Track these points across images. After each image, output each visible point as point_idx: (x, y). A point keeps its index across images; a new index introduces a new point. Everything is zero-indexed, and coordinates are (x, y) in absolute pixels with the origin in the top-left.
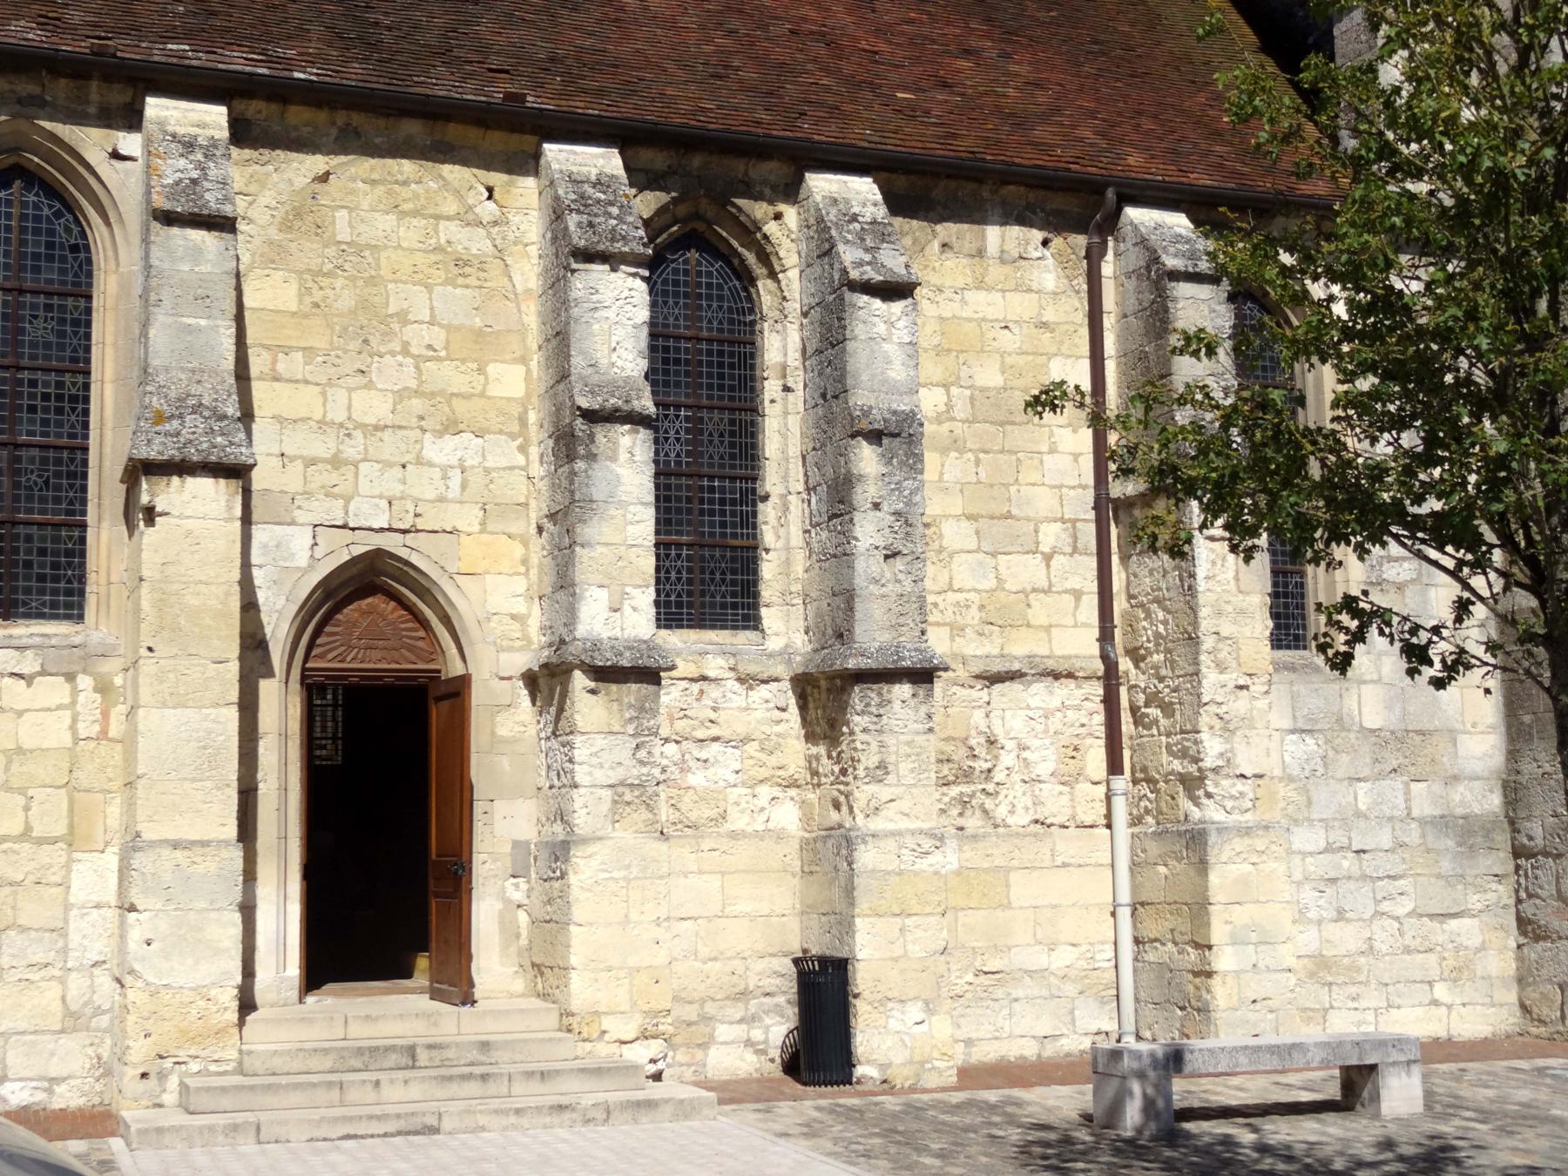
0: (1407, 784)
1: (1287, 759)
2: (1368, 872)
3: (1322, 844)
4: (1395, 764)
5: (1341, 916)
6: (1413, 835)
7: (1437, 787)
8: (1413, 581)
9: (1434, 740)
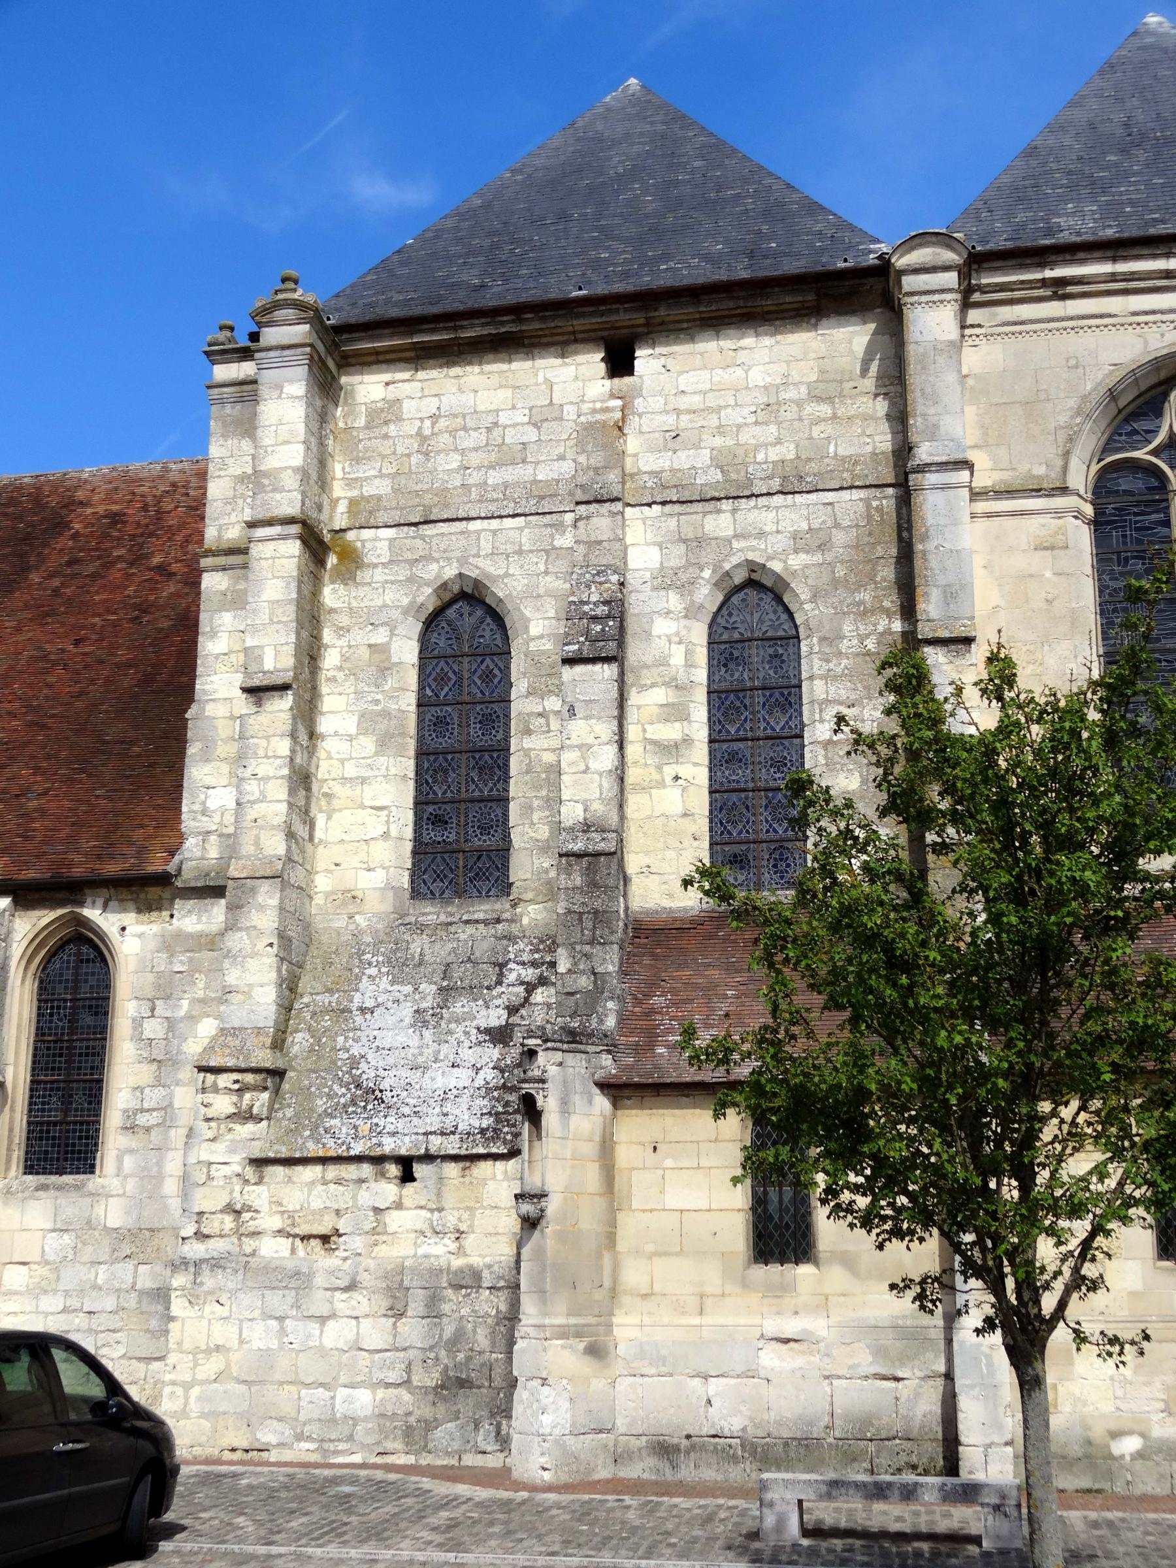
0: (136, 1267)
1: (46, 1248)
2: (94, 1327)
3: (61, 1307)
4: (128, 1252)
6: (132, 1301)
7: (158, 1268)
8: (158, 1125)
9: (161, 1235)
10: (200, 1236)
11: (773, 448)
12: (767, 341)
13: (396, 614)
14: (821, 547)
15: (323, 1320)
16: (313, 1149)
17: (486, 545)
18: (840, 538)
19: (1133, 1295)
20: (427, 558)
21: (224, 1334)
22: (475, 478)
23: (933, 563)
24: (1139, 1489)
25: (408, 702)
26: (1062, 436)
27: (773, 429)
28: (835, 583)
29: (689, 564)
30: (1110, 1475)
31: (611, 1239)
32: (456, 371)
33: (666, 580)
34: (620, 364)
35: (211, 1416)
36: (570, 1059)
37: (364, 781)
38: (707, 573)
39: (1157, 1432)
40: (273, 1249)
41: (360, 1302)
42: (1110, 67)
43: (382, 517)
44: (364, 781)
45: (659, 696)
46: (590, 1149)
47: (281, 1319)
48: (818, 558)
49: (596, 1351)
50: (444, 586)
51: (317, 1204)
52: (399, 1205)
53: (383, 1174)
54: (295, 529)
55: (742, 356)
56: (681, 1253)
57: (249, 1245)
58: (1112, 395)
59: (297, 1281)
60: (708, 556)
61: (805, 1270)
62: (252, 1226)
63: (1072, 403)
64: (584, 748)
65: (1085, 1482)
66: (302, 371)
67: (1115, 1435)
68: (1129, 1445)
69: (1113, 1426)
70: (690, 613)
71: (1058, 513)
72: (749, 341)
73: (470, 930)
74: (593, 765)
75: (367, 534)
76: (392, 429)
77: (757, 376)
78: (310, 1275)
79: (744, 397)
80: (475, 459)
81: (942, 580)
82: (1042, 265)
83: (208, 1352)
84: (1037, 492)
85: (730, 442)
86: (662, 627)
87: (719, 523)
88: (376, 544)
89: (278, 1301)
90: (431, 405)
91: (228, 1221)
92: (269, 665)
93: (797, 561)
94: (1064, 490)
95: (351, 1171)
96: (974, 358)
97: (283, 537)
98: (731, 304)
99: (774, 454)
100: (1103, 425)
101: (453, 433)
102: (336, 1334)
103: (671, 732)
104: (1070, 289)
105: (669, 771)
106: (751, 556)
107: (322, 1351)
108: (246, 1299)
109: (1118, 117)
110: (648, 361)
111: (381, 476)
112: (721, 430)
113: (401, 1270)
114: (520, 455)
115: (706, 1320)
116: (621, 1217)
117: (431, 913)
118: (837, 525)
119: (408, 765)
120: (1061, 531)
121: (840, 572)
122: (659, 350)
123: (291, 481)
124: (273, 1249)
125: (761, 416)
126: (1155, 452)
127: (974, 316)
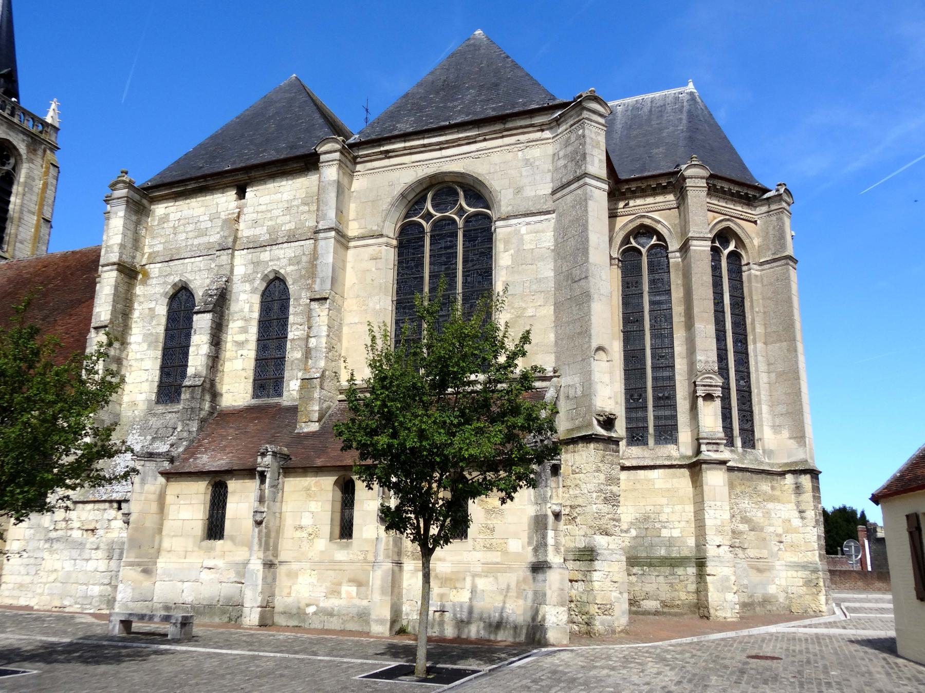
5: (28, 574)
10: (55, 530)
11: (288, 224)
12: (290, 182)
13: (158, 296)
14: (298, 263)
15: (87, 560)
16: (91, 498)
17: (189, 269)
18: (304, 259)
19: (322, 552)
20: (170, 274)
21: (57, 565)
22: (190, 242)
23: (319, 269)
24: (312, 626)
25: (161, 330)
26: (384, 213)
27: (288, 217)
28: (301, 277)
29: (254, 272)
30: (304, 621)
31: (160, 530)
32: (188, 201)
33: (247, 279)
34: (241, 194)
35: (51, 594)
36: (148, 464)
37: (142, 360)
38: (259, 275)
39: (322, 605)
40: (76, 534)
41: (100, 554)
42: (453, 55)
43: (158, 259)
44: (142, 360)
45: (240, 323)
46: (154, 497)
47: (75, 560)
48: (296, 267)
49: (147, 572)
50: (175, 284)
51: (91, 518)
52: (115, 519)
53: (111, 507)
54: (115, 267)
55: (281, 189)
56: (181, 536)
57: (69, 532)
58: (403, 195)
59: (80, 545)
60: (260, 269)
61: (221, 542)
62: (70, 526)
63: (389, 200)
64: (198, 346)
65: (296, 623)
66: (124, 207)
67: (308, 605)
68: (311, 610)
69: (307, 602)
70: (254, 291)
71: (379, 245)
72: (284, 183)
73: (170, 415)
74: (200, 352)
75: (152, 266)
76: (165, 225)
77: (286, 197)
78: (85, 544)
79: (280, 205)
80: (191, 235)
81: (321, 275)
82: (380, 146)
83: (52, 571)
84: (372, 237)
85: (273, 223)
86: (243, 297)
87: (265, 256)
88: (154, 270)
89: (75, 553)
90: (178, 215)
91: (64, 524)
92: (102, 319)
93: (290, 269)
94: (382, 236)
95: (102, 506)
96: (359, 184)
97: (112, 270)
98: (276, 169)
99: (287, 227)
100: (402, 207)
101: (184, 225)
102: (91, 565)
103: (241, 338)
104: (391, 154)
105: (240, 352)
106: (275, 268)
107: (86, 572)
108: (66, 553)
109: (443, 78)
110: (250, 193)
111: (160, 243)
112: (271, 219)
113: (113, 542)
114: (203, 233)
115: (186, 560)
116: (165, 522)
117: (161, 409)
118: (304, 254)
119: (159, 354)
120: (380, 252)
121: (303, 272)
122: (255, 188)
123: (116, 249)
124: (76, 534)
125: (285, 212)
126: (420, 218)
127: (359, 167)
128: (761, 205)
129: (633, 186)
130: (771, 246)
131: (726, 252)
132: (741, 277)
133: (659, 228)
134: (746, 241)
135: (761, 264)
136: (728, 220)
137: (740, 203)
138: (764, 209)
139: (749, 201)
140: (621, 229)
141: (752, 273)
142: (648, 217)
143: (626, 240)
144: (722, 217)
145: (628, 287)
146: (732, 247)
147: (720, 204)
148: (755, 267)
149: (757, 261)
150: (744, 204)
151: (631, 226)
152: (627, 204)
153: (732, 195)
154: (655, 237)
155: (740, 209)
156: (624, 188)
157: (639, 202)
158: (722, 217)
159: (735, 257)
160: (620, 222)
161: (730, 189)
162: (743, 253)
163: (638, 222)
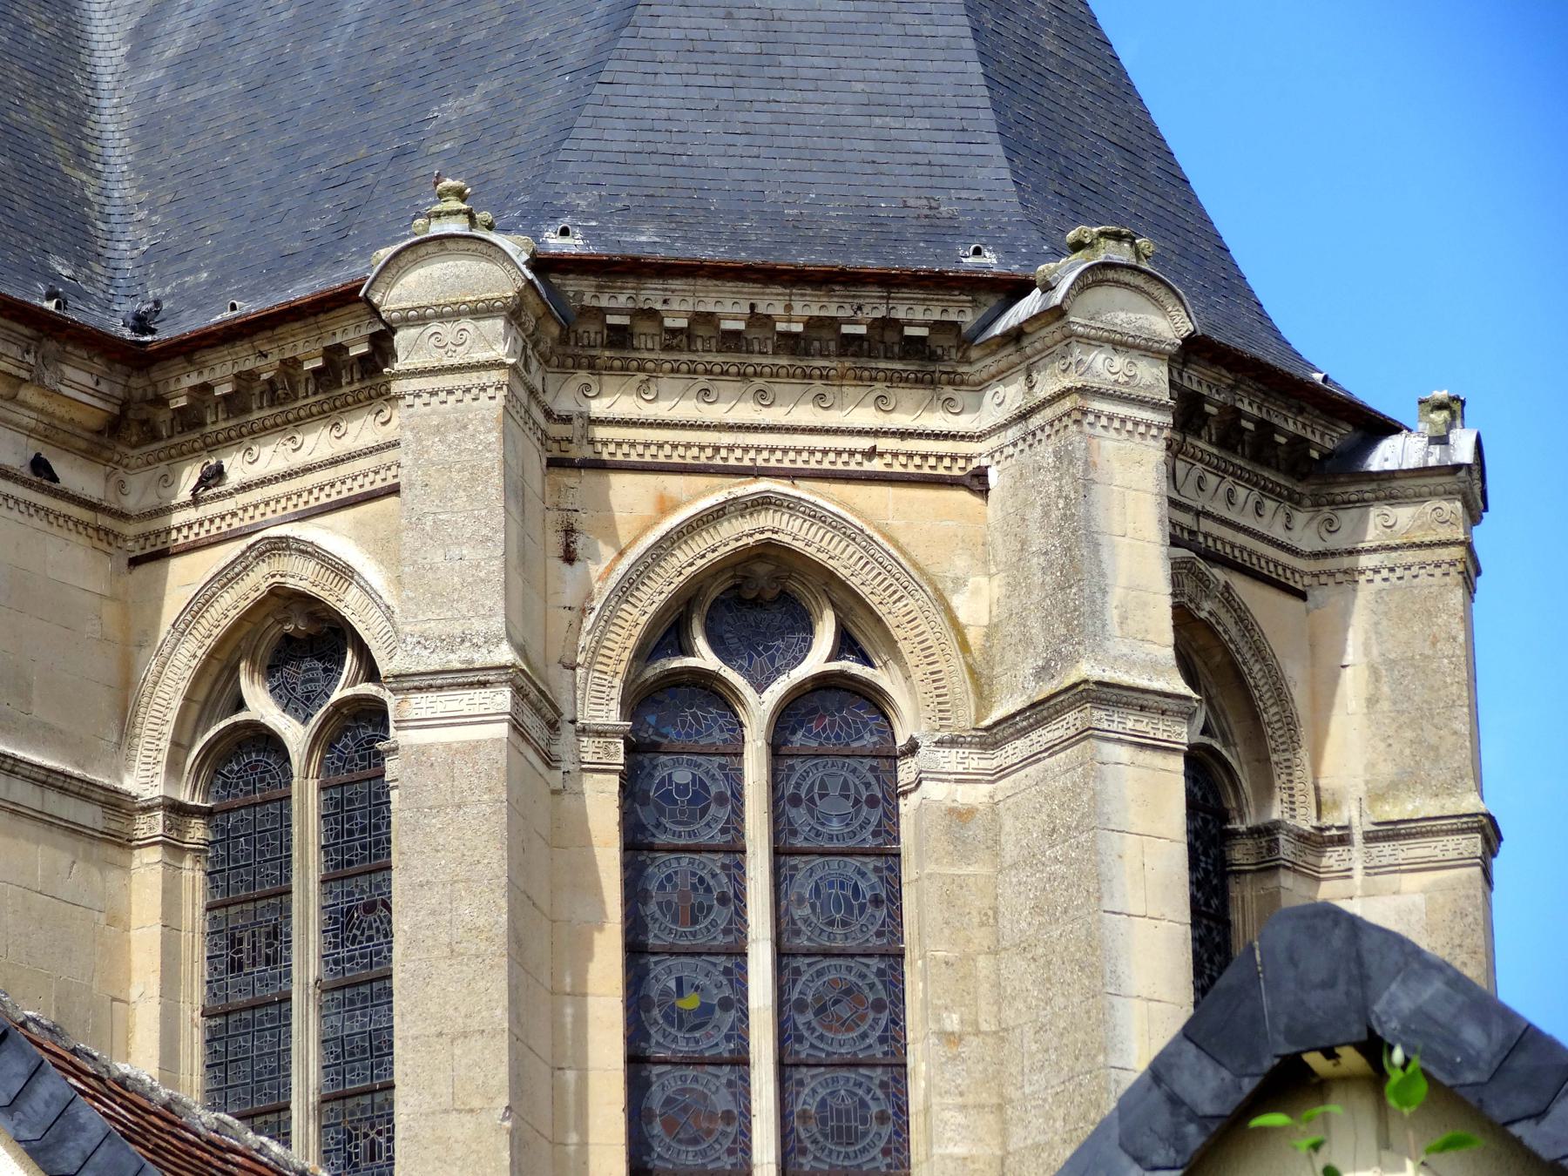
128: (1001, 376)
129: (221, 372)
130: (1036, 629)
131: (758, 707)
132: (889, 827)
133: (350, 605)
134: (892, 614)
135: (991, 737)
136: (763, 502)
137: (864, 379)
138: (1011, 395)
139: (929, 362)
140: (183, 627)
141: (937, 789)
142: (308, 551)
143: (215, 686)
144: (717, 492)
145: (236, 966)
146: (818, 659)
147: (716, 412)
148: (951, 759)
149: (964, 718)
150: (893, 379)
151: (231, 604)
152: (215, 475)
153: (792, 344)
154: (350, 659)
155: (865, 416)
156: (181, 385)
157: (272, 456)
158: (717, 492)
159: (840, 712)
160: (184, 577)
161: (757, 319)
162: (882, 677)
163: (257, 581)
